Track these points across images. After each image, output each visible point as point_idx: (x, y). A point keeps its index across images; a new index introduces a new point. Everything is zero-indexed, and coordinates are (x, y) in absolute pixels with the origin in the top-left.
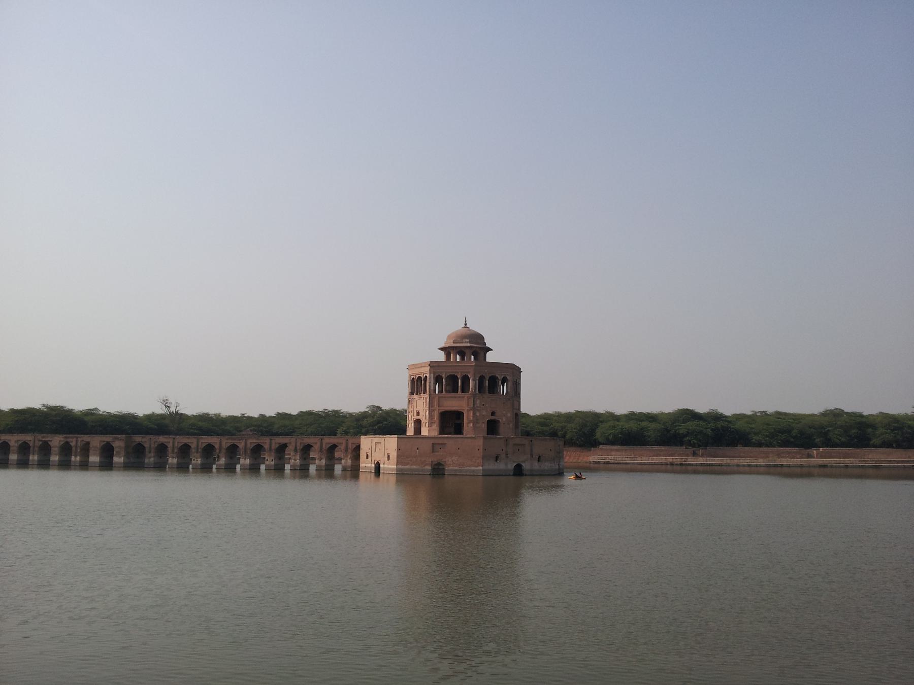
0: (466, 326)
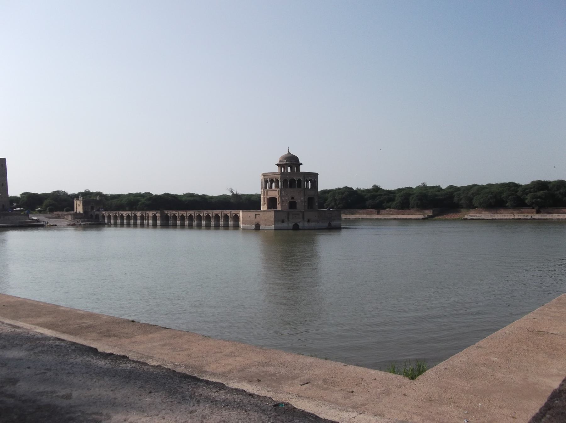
0: (289, 153)
